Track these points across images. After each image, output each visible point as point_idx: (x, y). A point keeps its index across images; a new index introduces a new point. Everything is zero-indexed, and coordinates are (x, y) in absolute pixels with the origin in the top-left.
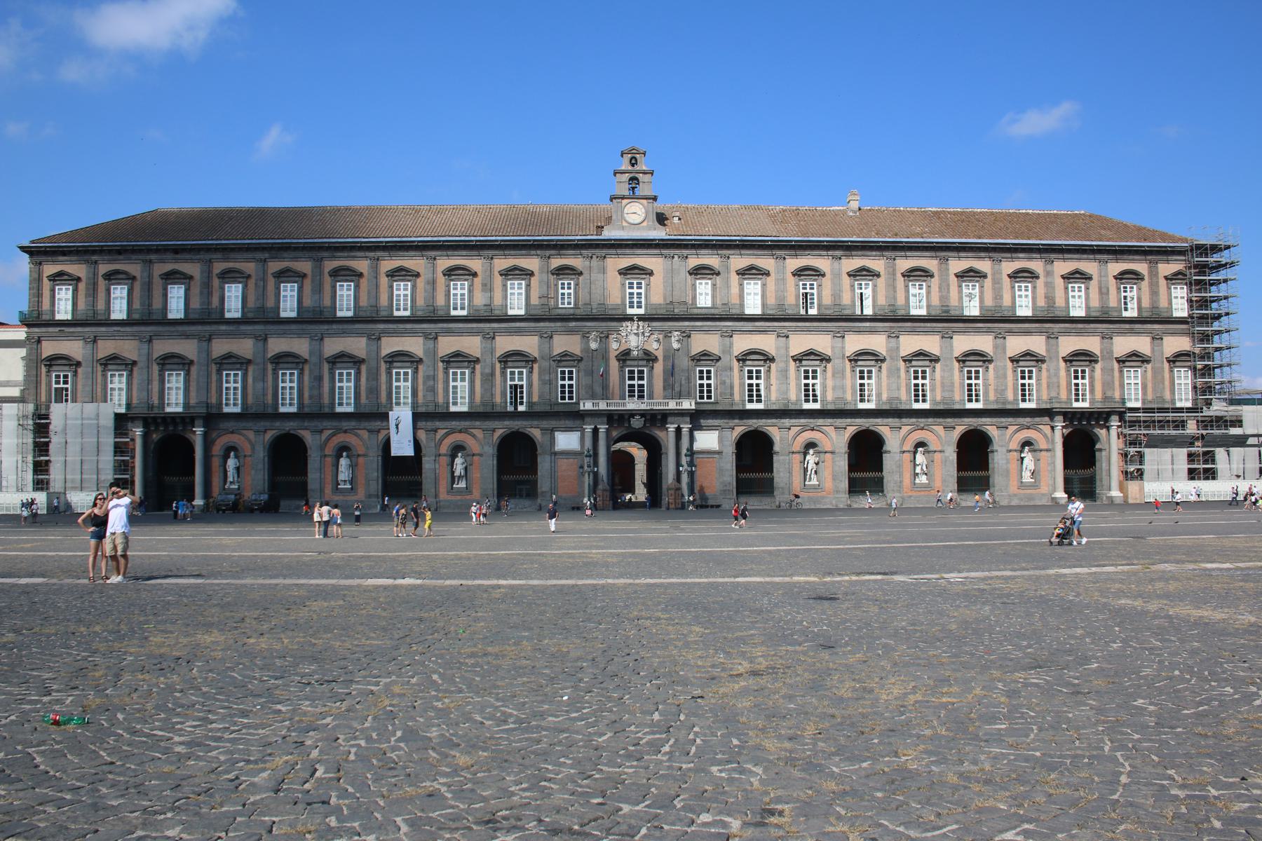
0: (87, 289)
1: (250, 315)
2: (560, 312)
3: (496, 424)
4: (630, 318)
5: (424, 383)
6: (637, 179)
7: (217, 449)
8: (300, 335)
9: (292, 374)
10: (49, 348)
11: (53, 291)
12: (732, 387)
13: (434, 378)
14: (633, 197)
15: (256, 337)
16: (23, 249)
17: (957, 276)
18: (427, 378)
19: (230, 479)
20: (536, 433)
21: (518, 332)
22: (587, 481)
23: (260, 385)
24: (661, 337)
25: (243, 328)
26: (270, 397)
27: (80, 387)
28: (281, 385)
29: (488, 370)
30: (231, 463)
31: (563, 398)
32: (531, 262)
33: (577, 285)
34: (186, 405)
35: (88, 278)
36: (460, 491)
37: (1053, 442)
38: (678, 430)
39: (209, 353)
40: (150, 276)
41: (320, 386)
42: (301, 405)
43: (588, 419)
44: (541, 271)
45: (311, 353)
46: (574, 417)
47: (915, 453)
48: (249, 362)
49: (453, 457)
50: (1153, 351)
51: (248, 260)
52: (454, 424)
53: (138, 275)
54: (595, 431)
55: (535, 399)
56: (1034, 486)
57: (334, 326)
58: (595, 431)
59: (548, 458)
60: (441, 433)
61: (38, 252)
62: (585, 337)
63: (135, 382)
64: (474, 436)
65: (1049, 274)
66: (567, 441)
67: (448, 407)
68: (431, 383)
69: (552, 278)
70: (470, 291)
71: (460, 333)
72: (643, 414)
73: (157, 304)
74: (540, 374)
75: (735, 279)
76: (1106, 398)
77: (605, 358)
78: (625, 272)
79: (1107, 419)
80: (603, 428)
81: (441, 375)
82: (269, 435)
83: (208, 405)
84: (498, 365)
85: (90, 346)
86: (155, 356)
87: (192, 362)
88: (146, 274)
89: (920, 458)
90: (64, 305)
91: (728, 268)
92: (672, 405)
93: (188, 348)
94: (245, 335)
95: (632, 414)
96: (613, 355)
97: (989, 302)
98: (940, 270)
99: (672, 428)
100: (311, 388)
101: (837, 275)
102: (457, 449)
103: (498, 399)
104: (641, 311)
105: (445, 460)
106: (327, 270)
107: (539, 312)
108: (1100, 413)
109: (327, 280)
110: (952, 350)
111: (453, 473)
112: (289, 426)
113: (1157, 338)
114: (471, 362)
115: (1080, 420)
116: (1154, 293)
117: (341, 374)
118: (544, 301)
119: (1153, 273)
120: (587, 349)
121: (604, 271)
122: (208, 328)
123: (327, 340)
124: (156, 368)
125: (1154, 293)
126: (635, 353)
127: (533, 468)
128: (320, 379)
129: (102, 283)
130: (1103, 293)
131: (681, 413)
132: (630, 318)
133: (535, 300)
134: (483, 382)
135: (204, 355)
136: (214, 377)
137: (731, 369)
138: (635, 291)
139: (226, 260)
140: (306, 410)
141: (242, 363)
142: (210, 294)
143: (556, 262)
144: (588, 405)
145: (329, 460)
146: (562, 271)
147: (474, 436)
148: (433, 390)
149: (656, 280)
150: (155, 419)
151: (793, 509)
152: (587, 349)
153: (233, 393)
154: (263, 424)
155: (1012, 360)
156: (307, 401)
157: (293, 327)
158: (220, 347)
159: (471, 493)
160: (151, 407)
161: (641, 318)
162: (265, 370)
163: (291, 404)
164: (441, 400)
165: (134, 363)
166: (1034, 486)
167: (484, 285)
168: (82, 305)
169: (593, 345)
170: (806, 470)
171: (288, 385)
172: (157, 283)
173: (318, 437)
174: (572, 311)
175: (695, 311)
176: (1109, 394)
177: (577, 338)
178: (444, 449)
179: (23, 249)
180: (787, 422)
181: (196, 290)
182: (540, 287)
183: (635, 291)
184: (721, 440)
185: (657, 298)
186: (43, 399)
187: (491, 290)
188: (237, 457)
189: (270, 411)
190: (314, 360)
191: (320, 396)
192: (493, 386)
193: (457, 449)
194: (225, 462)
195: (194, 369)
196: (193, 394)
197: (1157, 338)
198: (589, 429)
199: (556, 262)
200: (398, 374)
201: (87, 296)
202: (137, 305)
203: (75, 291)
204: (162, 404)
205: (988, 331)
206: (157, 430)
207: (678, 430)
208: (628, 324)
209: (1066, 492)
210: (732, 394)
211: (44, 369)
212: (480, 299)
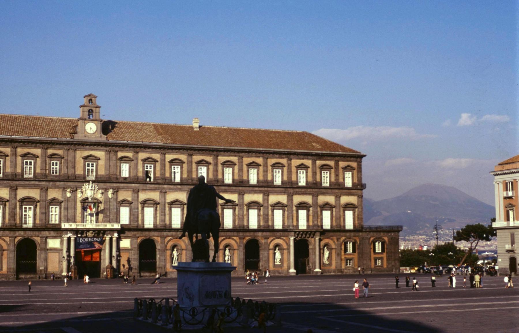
3: (17, 233)
4: (88, 181)
6: (92, 110)
11: (248, 171)
12: (137, 218)
14: (90, 120)
17: (247, 165)
20: (37, 239)
22: (65, 264)
24: (103, 191)
32: (37, 151)
33: (60, 163)
37: (288, 245)
38: (111, 239)
47: (225, 250)
50: (335, 202)
54: (69, 239)
56: (281, 266)
58: (69, 239)
62: (64, 189)
64: (4, 240)
65: (290, 165)
66: (54, 243)
69: (48, 160)
72: (94, 230)
74: (40, 208)
75: (140, 163)
76: (314, 226)
78: (86, 158)
79: (314, 235)
84: (18, 204)
89: (227, 252)
91: (137, 159)
92: (109, 226)
95: (88, 230)
97: (261, 178)
98: (238, 162)
99: (107, 238)
101: (190, 163)
108: (311, 232)
110: (243, 201)
113: (338, 198)
115: (302, 235)
116: (337, 175)
118: (43, 171)
119: (337, 165)
125: (337, 175)
126: (90, 199)
127: (34, 257)
130: (314, 173)
131: (112, 231)
133: (38, 171)
137: (137, 208)
138: (90, 168)
143: (50, 151)
144: (65, 225)
146: (52, 156)
147: (4, 240)
149: (101, 163)
155: (271, 206)
166: (281, 266)
170: (173, 259)
176: (316, 222)
180: (165, 233)
183: (90, 168)
185: (102, 172)
197: (338, 198)
199: (50, 151)
205: (260, 192)
207: (111, 239)
208: (87, 184)
209: (295, 269)
210: (137, 221)
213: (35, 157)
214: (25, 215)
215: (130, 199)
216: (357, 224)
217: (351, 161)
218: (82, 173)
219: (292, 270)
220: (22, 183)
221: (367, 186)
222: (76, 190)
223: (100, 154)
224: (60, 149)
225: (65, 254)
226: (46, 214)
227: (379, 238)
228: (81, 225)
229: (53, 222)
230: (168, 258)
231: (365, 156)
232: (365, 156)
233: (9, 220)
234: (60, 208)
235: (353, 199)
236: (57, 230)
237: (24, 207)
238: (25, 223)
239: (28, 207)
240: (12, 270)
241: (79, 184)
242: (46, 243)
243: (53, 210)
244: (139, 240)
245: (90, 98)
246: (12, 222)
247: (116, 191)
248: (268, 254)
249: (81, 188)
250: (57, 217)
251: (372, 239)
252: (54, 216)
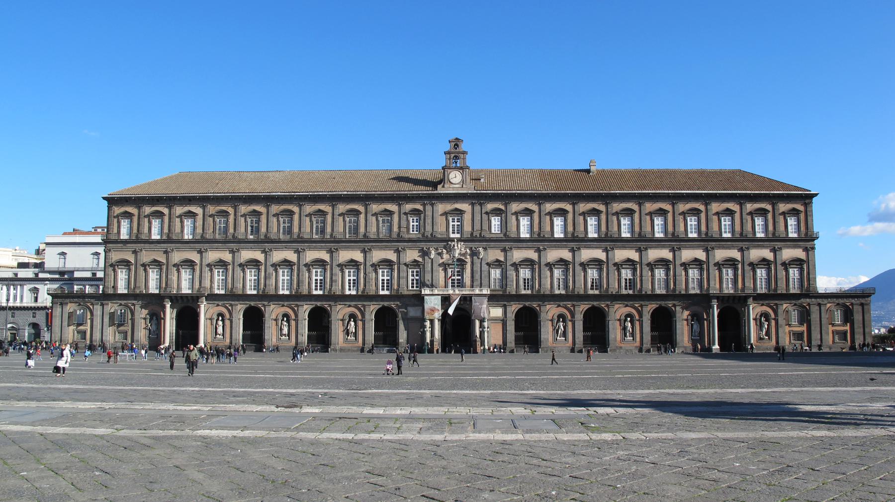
2: (411, 236)
10: (115, 256)
16: (104, 198)
31: (413, 287)
47: (625, 320)
61: (112, 201)
92: (477, 292)
93: (195, 257)
104: (458, 236)
132: (452, 240)
149: (467, 217)
161: (459, 240)
175: (492, 236)
179: (104, 198)
184: (505, 313)
215: (502, 259)
217: (796, 203)
219: (716, 347)
221: (820, 235)
223: (465, 206)
227: (838, 304)
230: (551, 329)
231: (816, 195)
232: (816, 195)
235: (799, 253)
244: (514, 308)
245: (456, 143)
247: (485, 249)
248: (682, 325)
251: (829, 305)
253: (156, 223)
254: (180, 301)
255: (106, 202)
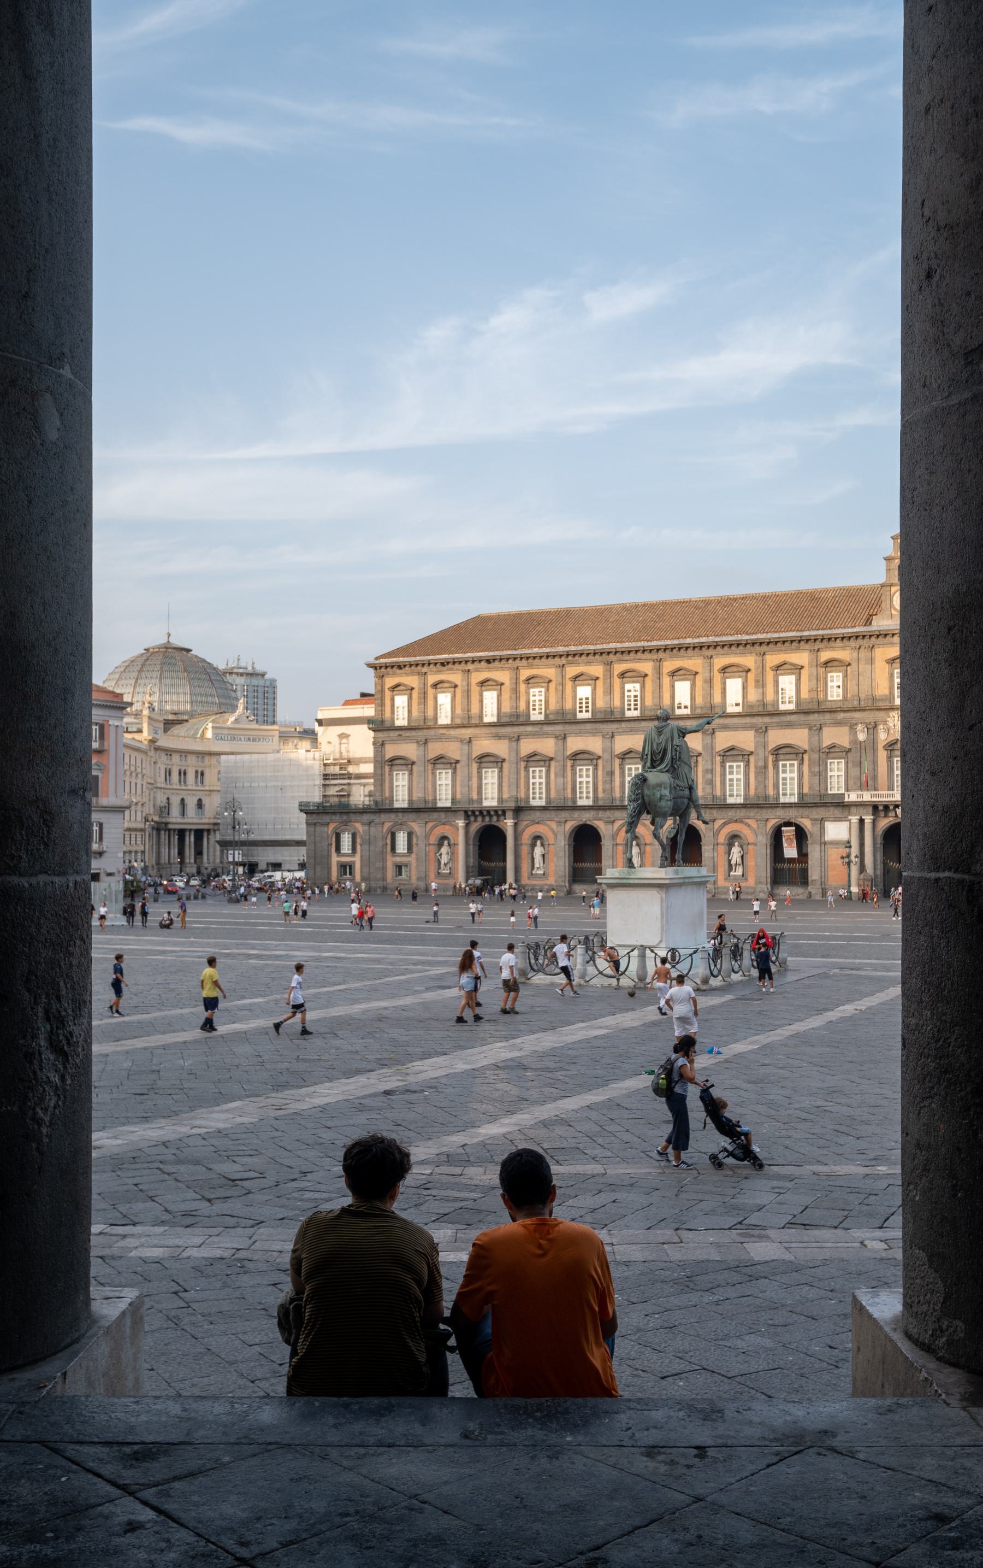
0: (419, 698)
1: (551, 717)
5: (703, 777)
7: (526, 838)
8: (594, 734)
9: (587, 770)
10: (391, 751)
13: (712, 771)
15: (556, 737)
18: (706, 771)
19: (537, 865)
20: (806, 824)
21: (790, 725)
23: (560, 780)
25: (547, 728)
26: (569, 791)
27: (415, 784)
28: (578, 780)
29: (761, 763)
30: (538, 851)
32: (801, 657)
34: (500, 800)
35: (420, 689)
36: (736, 878)
39: (517, 752)
40: (469, 685)
41: (612, 781)
42: (596, 798)
43: (853, 810)
44: (810, 666)
45: (604, 751)
46: (840, 806)
48: (551, 759)
49: (730, 845)
51: (548, 666)
52: (731, 814)
53: (458, 683)
54: (862, 821)
55: (806, 790)
57: (624, 725)
58: (862, 821)
59: (817, 848)
60: (718, 823)
61: (380, 668)
62: (852, 727)
63: (459, 778)
66: (837, 831)
67: (725, 799)
68: (710, 776)
70: (745, 688)
71: (735, 728)
73: (475, 710)
77: (875, 750)
80: (868, 819)
81: (718, 769)
82: (570, 826)
83: (517, 799)
84: (771, 758)
85: (422, 748)
86: (474, 756)
87: (504, 760)
88: (465, 683)
90: (401, 710)
94: (547, 735)
96: (880, 746)
100: (604, 782)
102: (734, 838)
103: (617, 794)
105: (722, 849)
106: (616, 673)
107: (810, 706)
109: (617, 681)
111: (730, 861)
112: (586, 818)
114: (745, 756)
117: (784, 766)
120: (855, 741)
121: (872, 661)
122: (516, 729)
123: (617, 738)
124: (475, 766)
128: (612, 773)
129: (431, 692)
133: (805, 695)
134: (757, 774)
135: (514, 754)
136: (523, 773)
139: (531, 666)
140: (600, 803)
141: (545, 761)
142: (518, 698)
143: (825, 656)
144: (853, 797)
145: (620, 848)
148: (711, 783)
150: (473, 812)
151: (522, 895)
152: (855, 741)
153: (538, 788)
154: (565, 815)
156: (601, 795)
157: (588, 726)
158: (527, 746)
159: (746, 880)
160: (471, 801)
162: (564, 766)
163: (587, 798)
164: (718, 793)
165: (457, 762)
167: (757, 681)
168: (415, 713)
169: (862, 737)
171: (584, 779)
172: (475, 689)
173: (610, 827)
174: (840, 704)
177: (846, 729)
178: (722, 838)
181: (506, 695)
182: (810, 680)
186: (387, 795)
187: (763, 686)
188: (542, 845)
189: (570, 804)
190: (607, 756)
191: (612, 789)
192: (765, 778)
193: (734, 838)
194: (533, 850)
195: (505, 765)
196: (505, 789)
198: (855, 819)
200: (731, 767)
201: (419, 704)
202: (458, 711)
203: (410, 699)
204: (480, 800)
206: (475, 821)
211: (387, 769)
212: (753, 696)
213: (797, 669)
214: (784, 779)
216: (752, 792)
218: (887, 692)
220: (776, 719)
222: (876, 726)
224: (844, 648)
225: (855, 851)
226: (821, 775)
228: (888, 796)
229: (835, 791)
233: (756, 789)
234: (847, 763)
236: (840, 806)
237: (781, 763)
238: (784, 795)
239: (788, 763)
240: (764, 880)
241: (882, 714)
242: (822, 830)
243: (835, 766)
246: (708, 790)
249: (885, 722)
250: (843, 780)
252: (444, 787)
253: (444, 699)
254: (480, 819)
255: (372, 670)
